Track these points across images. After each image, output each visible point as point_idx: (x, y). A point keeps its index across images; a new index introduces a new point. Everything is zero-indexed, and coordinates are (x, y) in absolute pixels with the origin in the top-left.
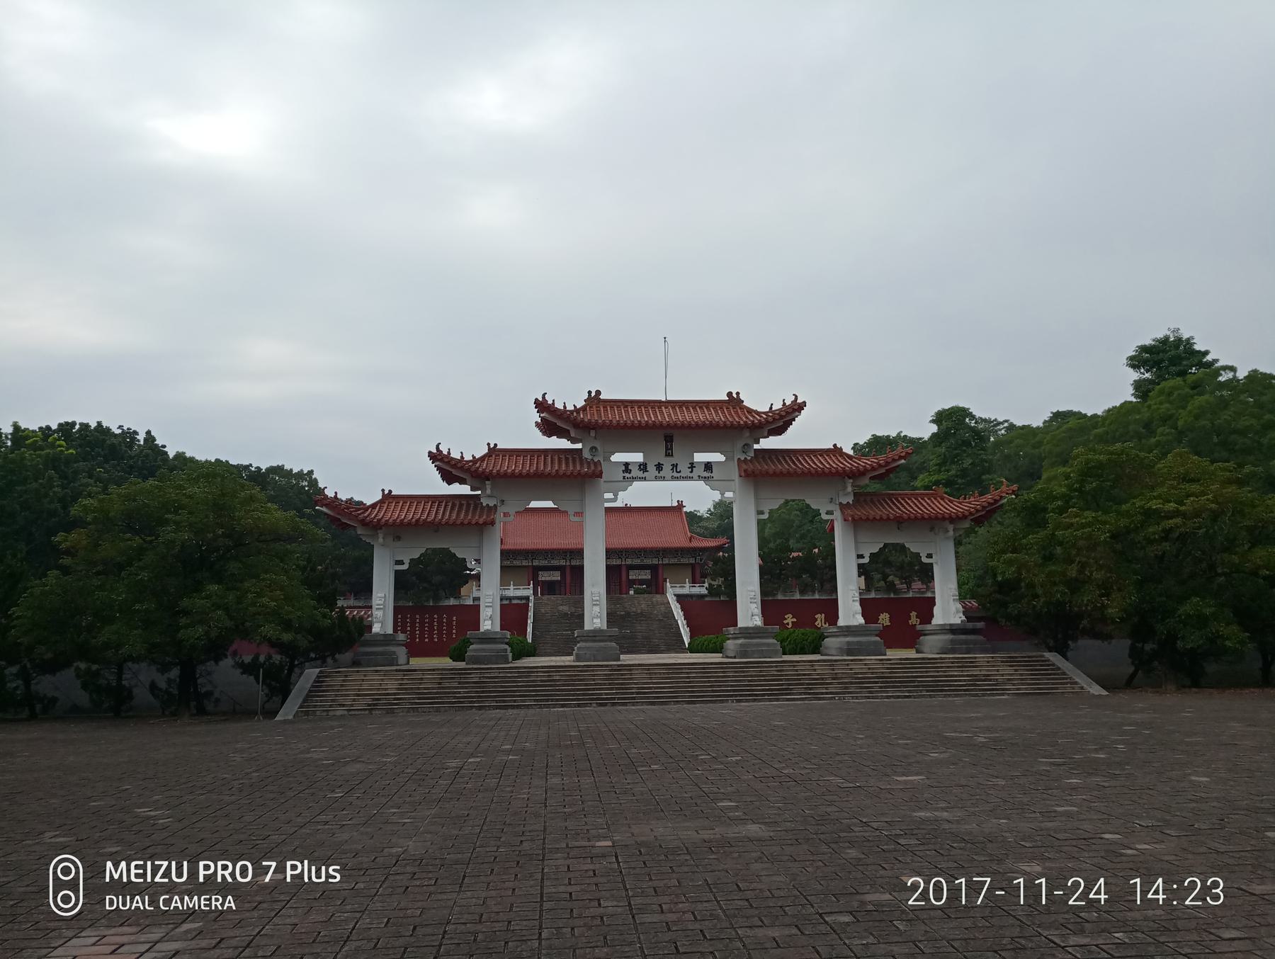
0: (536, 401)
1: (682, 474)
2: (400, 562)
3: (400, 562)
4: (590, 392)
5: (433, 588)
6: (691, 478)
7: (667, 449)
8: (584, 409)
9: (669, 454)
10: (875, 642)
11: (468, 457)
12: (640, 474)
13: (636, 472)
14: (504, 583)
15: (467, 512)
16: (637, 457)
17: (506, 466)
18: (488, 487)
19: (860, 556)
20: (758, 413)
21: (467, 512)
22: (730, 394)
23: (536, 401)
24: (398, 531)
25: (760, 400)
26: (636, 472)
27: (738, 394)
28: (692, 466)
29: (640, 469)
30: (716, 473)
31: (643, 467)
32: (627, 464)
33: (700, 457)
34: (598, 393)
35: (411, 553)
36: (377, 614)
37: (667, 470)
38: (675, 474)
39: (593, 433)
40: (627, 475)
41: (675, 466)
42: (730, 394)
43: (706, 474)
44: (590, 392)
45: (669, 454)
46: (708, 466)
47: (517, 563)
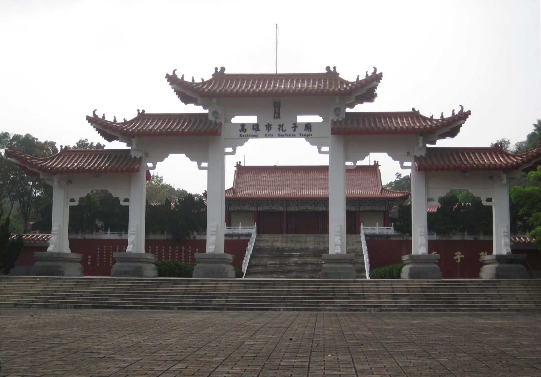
0: (167, 76)
1: (287, 132)
2: (72, 200)
3: (72, 200)
4: (216, 69)
5: (99, 217)
6: (294, 136)
7: (275, 113)
8: (209, 82)
9: (277, 116)
10: (350, 268)
11: (120, 120)
12: (254, 133)
13: (250, 131)
14: (229, 221)
15: (117, 162)
16: (252, 119)
17: (150, 127)
18: (134, 143)
19: (429, 200)
20: (347, 83)
21: (117, 162)
22: (328, 68)
23: (167, 76)
24: (70, 176)
25: (351, 73)
26: (250, 131)
27: (335, 68)
28: (295, 126)
29: (253, 129)
30: (314, 132)
31: (256, 127)
32: (243, 125)
33: (302, 119)
34: (223, 69)
35: (80, 193)
36: (131, 238)
37: (275, 128)
38: (281, 133)
39: (214, 100)
40: (243, 133)
41: (281, 127)
42: (328, 68)
43: (306, 133)
44: (216, 69)
45: (277, 116)
46: (308, 126)
47: (244, 208)
